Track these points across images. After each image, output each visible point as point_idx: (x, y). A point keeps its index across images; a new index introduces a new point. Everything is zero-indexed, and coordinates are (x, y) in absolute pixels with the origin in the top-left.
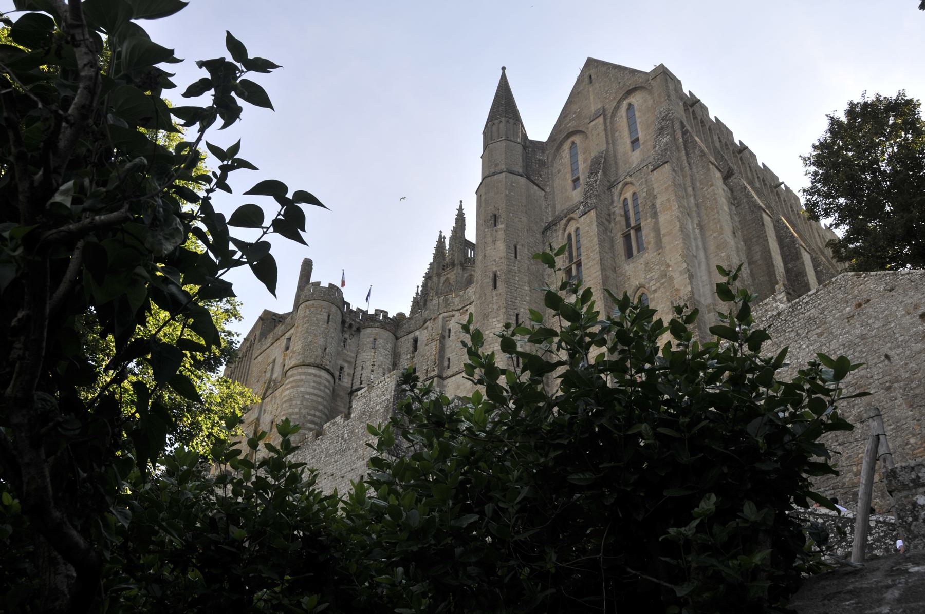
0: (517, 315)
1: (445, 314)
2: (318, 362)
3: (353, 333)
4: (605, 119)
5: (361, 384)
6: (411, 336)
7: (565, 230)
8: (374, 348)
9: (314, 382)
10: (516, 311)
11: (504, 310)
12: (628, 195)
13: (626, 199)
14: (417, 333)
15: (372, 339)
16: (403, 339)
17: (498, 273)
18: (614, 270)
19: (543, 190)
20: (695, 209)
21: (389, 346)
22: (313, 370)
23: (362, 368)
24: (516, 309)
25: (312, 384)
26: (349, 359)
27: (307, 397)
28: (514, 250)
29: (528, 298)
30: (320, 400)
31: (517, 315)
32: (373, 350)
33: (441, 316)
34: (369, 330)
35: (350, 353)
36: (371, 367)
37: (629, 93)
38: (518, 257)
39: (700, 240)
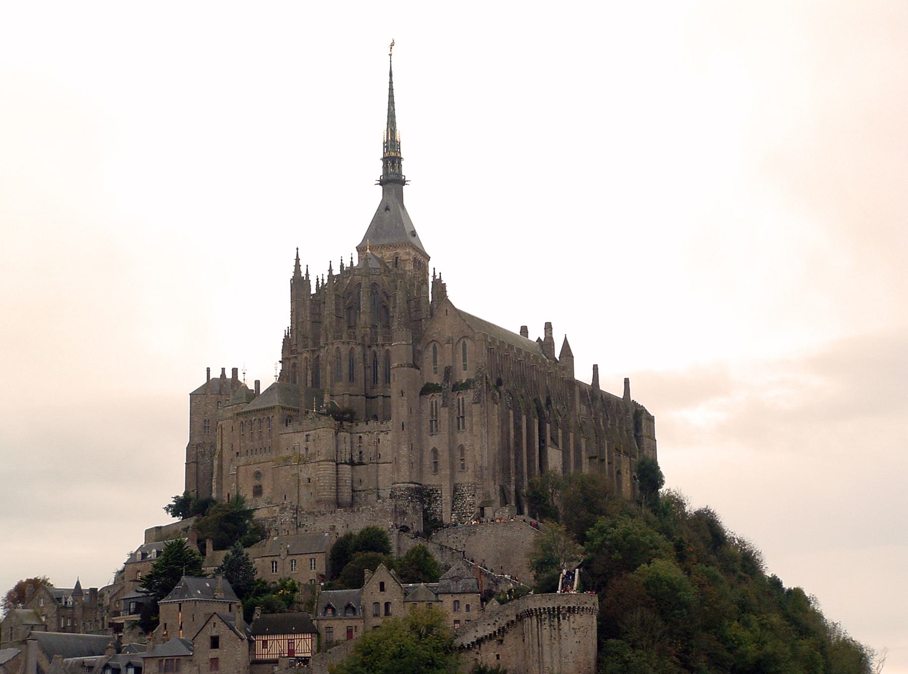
4: (453, 346)
6: (359, 435)
7: (430, 399)
8: (345, 443)
12: (461, 398)
13: (459, 399)
14: (362, 435)
16: (354, 435)
17: (404, 424)
18: (452, 434)
19: (419, 369)
20: (486, 424)
23: (341, 453)
33: (375, 433)
34: (342, 433)
37: (465, 337)
39: (486, 438)
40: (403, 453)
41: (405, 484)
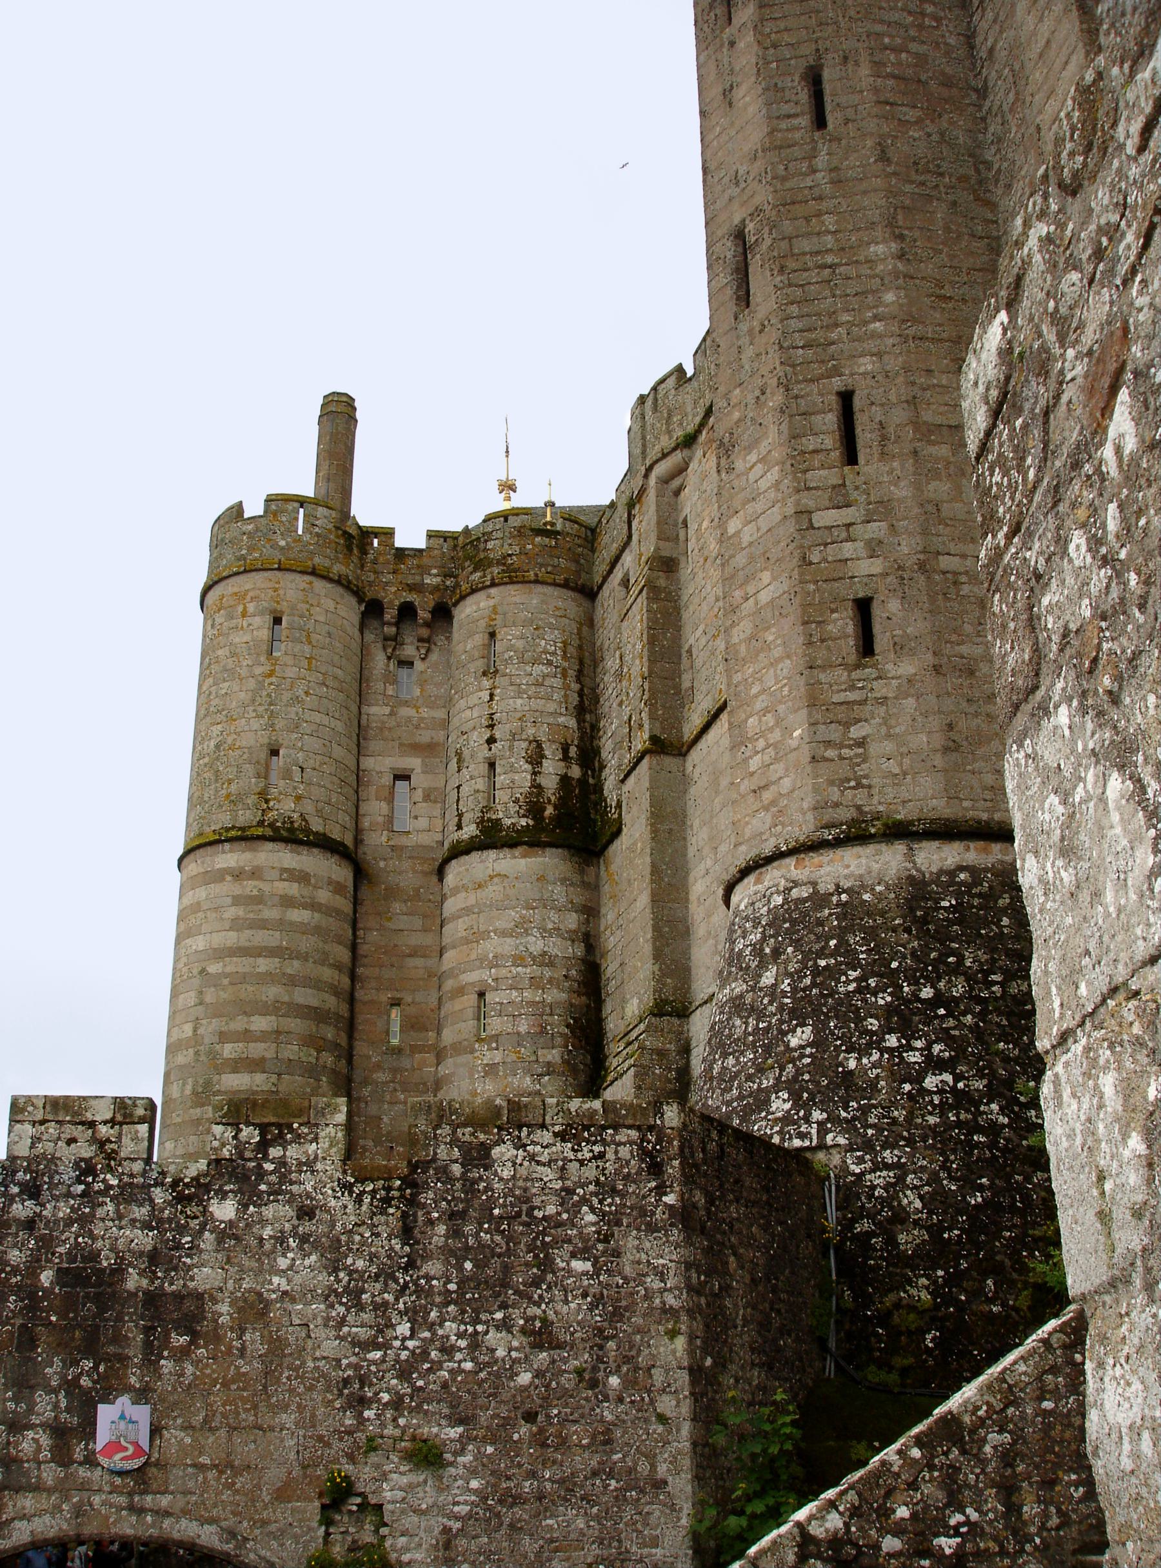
0: (846, 398)
1: (661, 469)
2: (246, 817)
3: (424, 632)
5: (459, 827)
6: (618, 574)
8: (490, 672)
9: (237, 901)
10: (837, 383)
11: (776, 399)
15: (480, 639)
17: (750, 227)
21: (550, 642)
22: (229, 858)
24: (836, 372)
25: (231, 912)
26: (425, 737)
27: (214, 968)
28: (804, 96)
29: (890, 297)
30: (264, 965)
31: (846, 398)
32: (486, 683)
35: (425, 712)
36: (484, 752)
38: (831, 120)
40: (746, 539)
41: (774, 875)
